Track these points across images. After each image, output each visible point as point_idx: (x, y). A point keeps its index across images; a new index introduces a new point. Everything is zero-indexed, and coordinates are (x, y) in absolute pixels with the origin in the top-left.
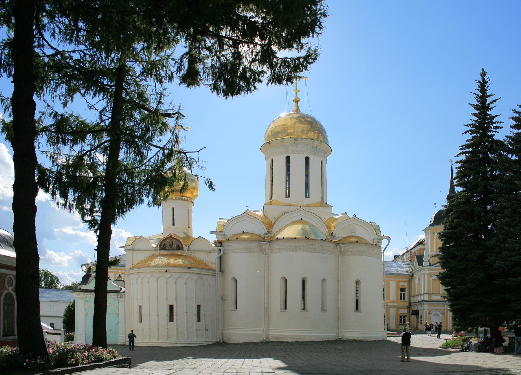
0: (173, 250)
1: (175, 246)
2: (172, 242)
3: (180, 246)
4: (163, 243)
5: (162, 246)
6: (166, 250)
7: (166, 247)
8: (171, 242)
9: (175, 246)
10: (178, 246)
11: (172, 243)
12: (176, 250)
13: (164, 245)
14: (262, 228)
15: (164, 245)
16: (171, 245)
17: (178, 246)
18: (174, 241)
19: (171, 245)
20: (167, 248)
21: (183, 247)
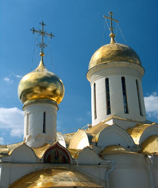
0: (58, 163)
1: (61, 159)
3: (67, 159)
4: (48, 154)
5: (46, 157)
6: (51, 163)
7: (51, 159)
9: (61, 158)
10: (64, 157)
11: (58, 154)
12: (62, 163)
13: (49, 156)
14: (129, 141)
15: (49, 156)
16: (56, 157)
17: (64, 157)
18: (60, 151)
19: (56, 157)
20: (52, 161)
21: (69, 159)
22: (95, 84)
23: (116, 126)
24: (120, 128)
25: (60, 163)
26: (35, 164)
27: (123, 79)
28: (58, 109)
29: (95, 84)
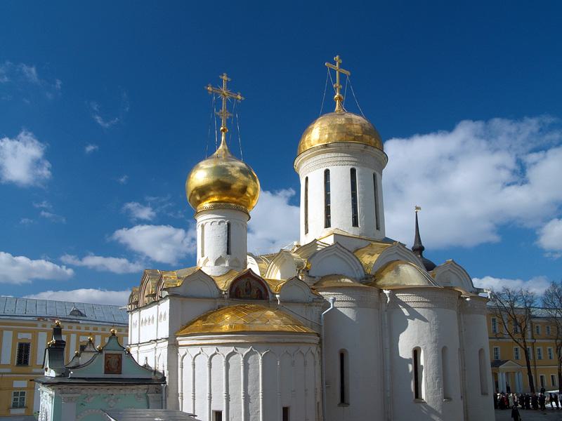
2: (250, 284)
3: (263, 292)
5: (234, 291)
6: (240, 298)
8: (248, 284)
9: (254, 292)
10: (259, 291)
12: (256, 299)
13: (237, 289)
15: (237, 289)
16: (248, 290)
17: (259, 291)
18: (253, 282)
19: (248, 290)
20: (242, 296)
21: (267, 294)
22: (307, 178)
23: (339, 247)
24: (344, 250)
25: (253, 299)
26: (217, 300)
27: (353, 171)
28: (250, 218)
29: (307, 178)
